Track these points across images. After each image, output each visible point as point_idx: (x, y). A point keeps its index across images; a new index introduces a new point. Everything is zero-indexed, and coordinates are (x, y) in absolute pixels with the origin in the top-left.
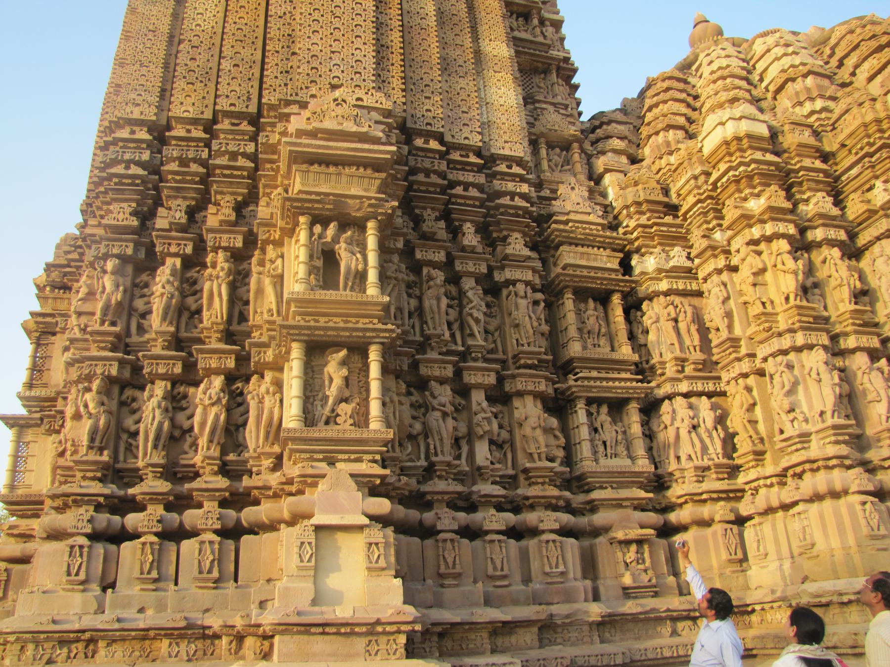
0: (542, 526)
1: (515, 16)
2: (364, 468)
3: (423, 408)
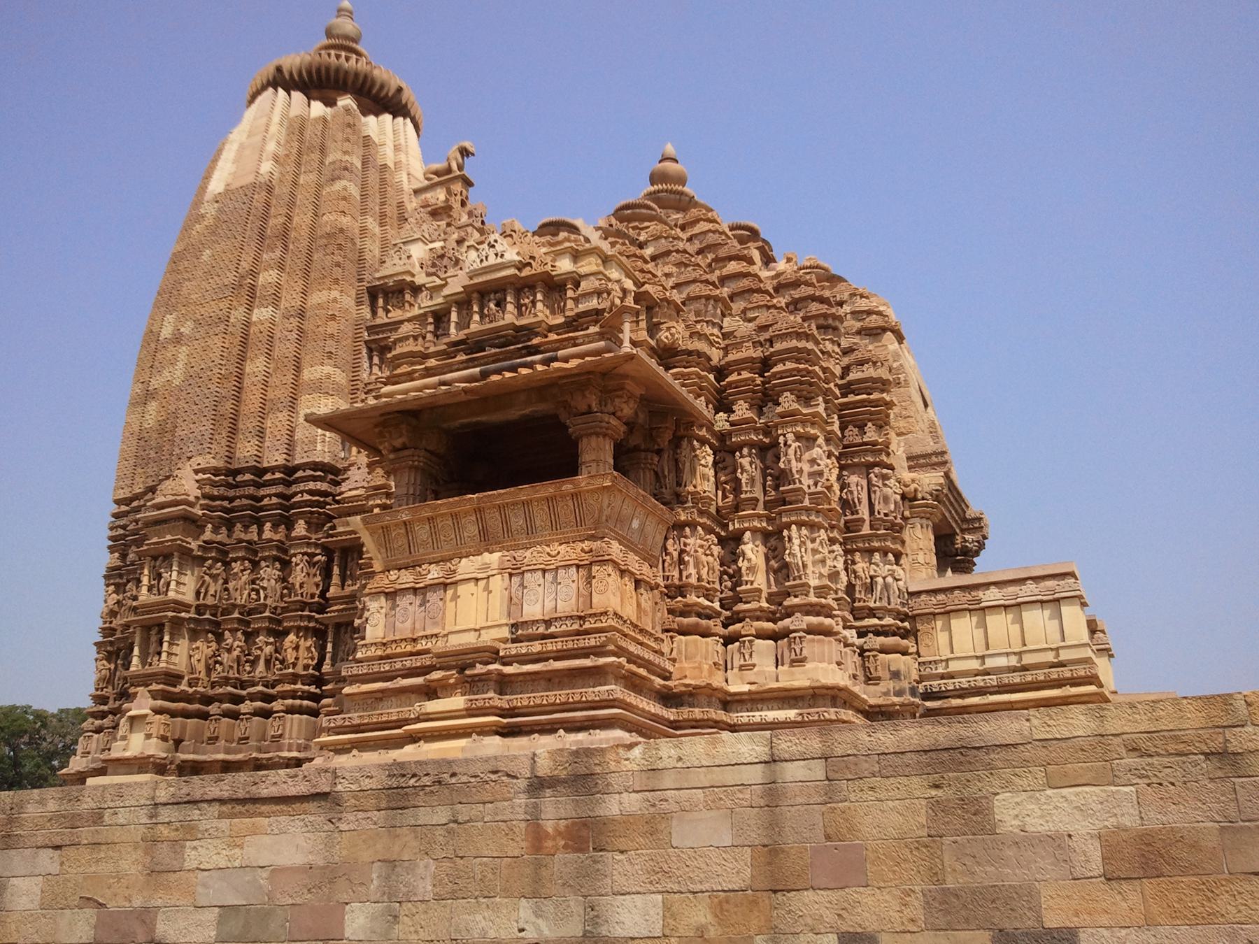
2: (154, 687)
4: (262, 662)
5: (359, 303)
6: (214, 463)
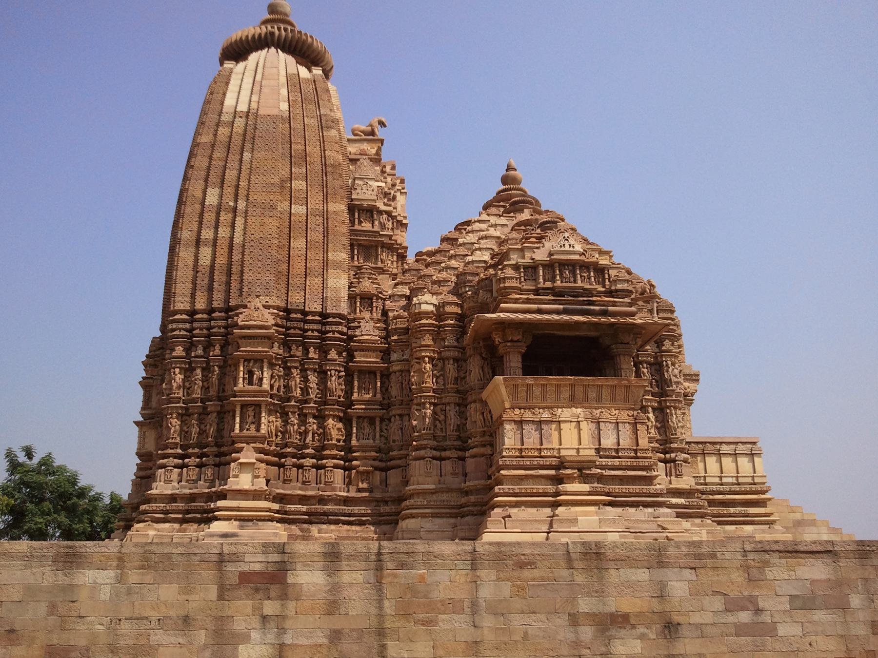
3: (286, 422)
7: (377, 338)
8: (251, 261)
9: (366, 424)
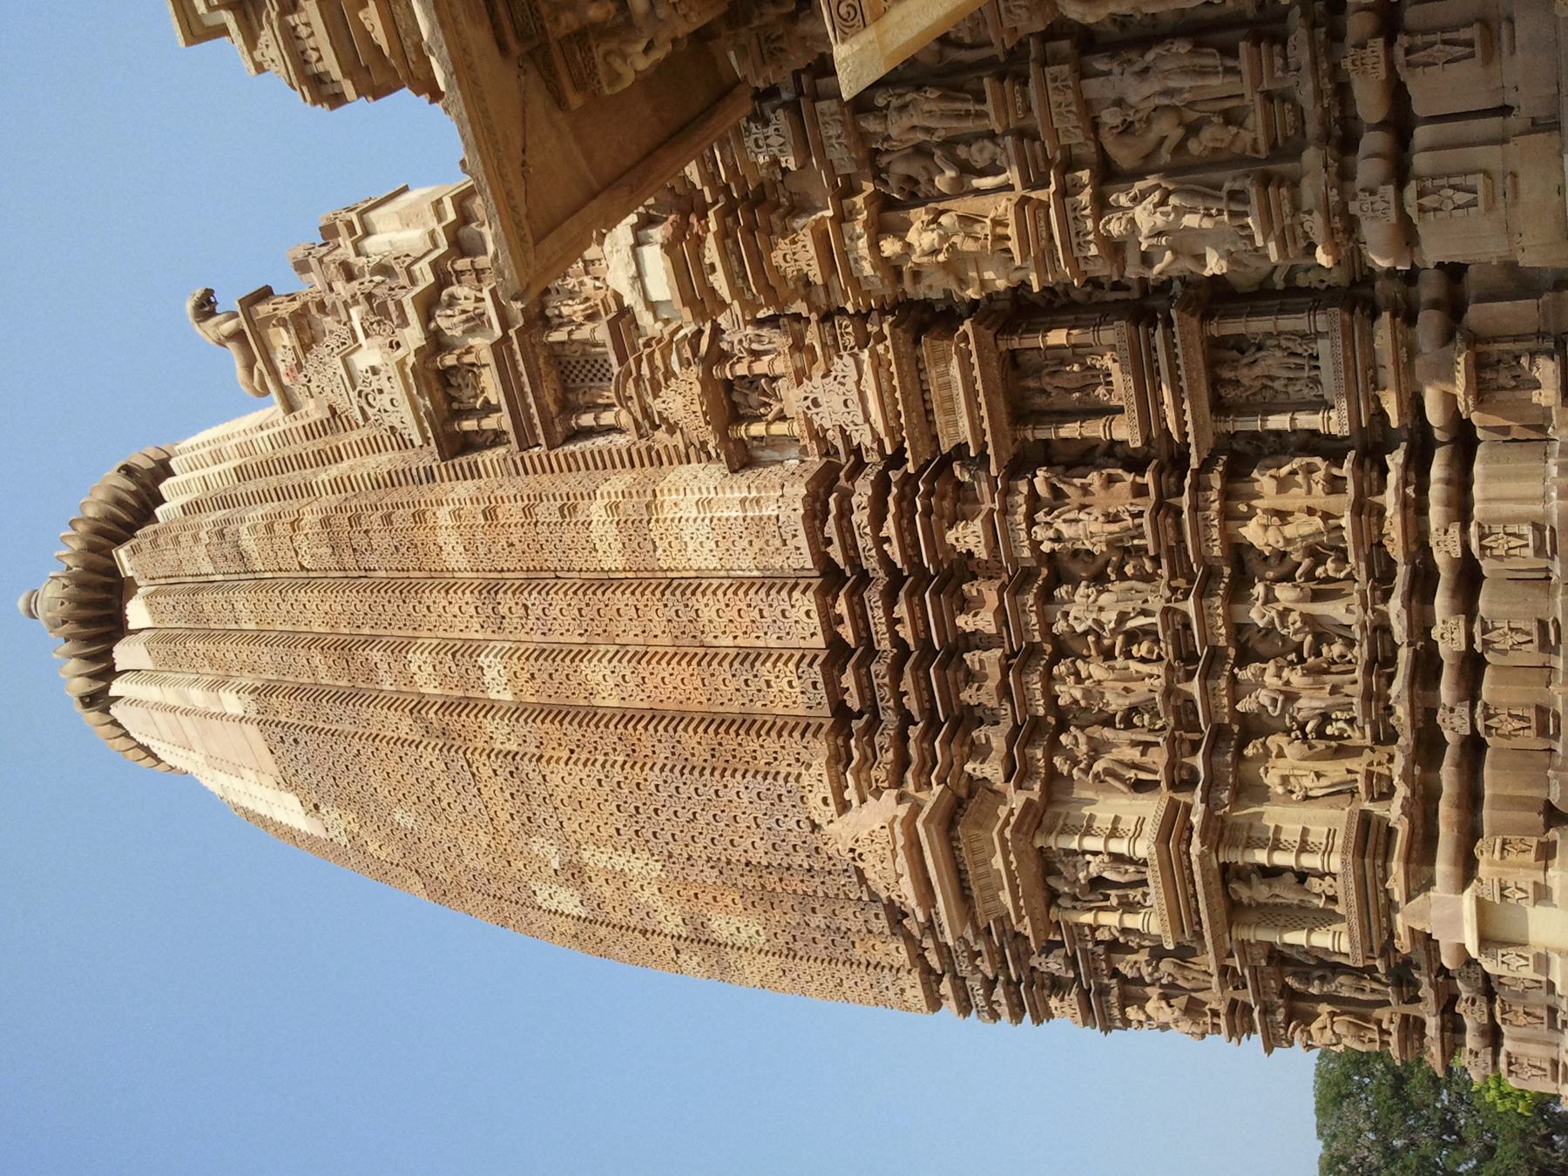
0: (1457, 552)
1: (453, 392)
4: (1319, 609)
5: (474, 472)
6: (819, 765)
7: (865, 355)
8: (703, 841)
9: (1245, 375)
